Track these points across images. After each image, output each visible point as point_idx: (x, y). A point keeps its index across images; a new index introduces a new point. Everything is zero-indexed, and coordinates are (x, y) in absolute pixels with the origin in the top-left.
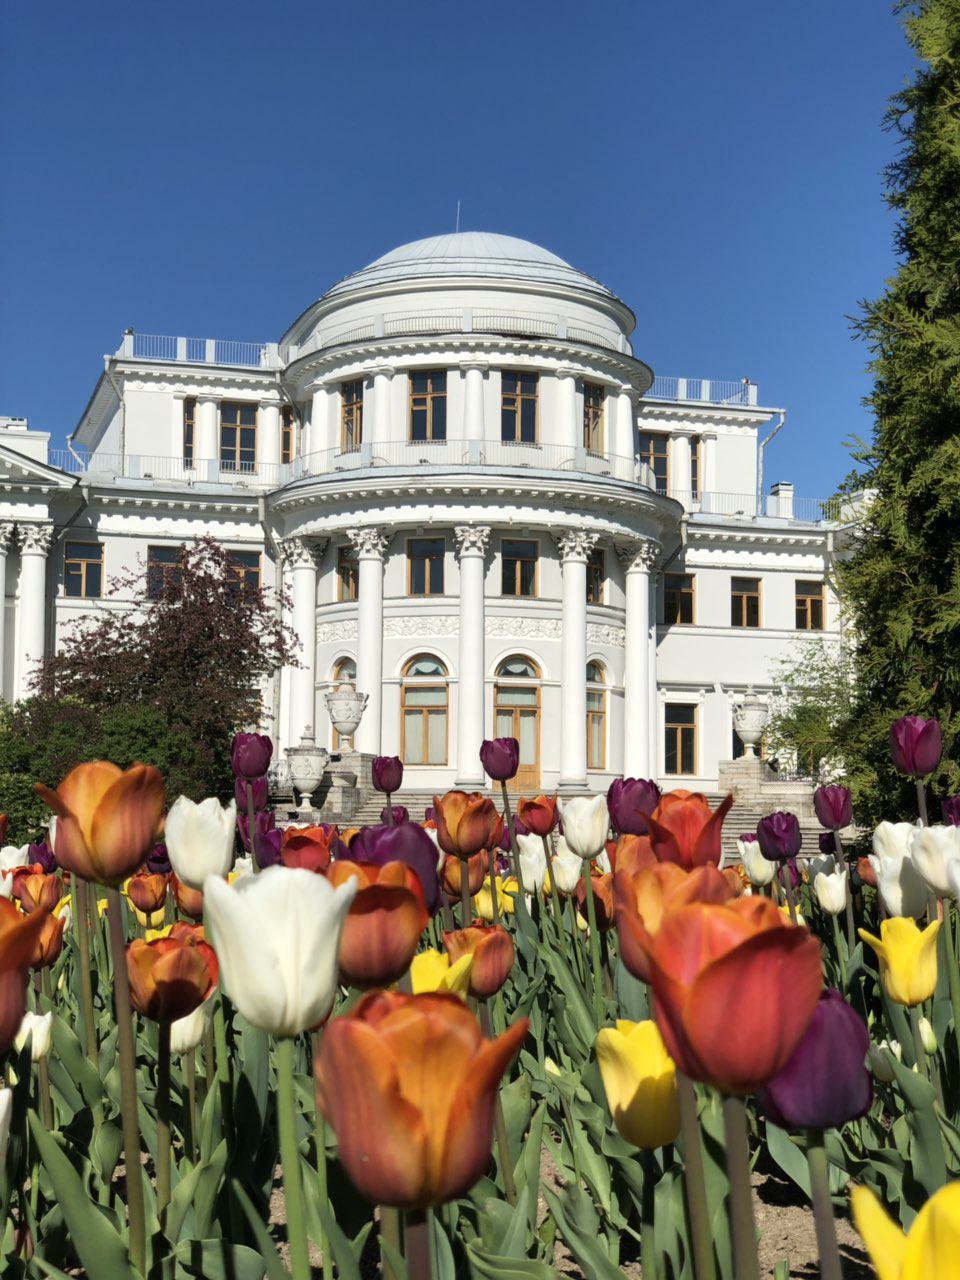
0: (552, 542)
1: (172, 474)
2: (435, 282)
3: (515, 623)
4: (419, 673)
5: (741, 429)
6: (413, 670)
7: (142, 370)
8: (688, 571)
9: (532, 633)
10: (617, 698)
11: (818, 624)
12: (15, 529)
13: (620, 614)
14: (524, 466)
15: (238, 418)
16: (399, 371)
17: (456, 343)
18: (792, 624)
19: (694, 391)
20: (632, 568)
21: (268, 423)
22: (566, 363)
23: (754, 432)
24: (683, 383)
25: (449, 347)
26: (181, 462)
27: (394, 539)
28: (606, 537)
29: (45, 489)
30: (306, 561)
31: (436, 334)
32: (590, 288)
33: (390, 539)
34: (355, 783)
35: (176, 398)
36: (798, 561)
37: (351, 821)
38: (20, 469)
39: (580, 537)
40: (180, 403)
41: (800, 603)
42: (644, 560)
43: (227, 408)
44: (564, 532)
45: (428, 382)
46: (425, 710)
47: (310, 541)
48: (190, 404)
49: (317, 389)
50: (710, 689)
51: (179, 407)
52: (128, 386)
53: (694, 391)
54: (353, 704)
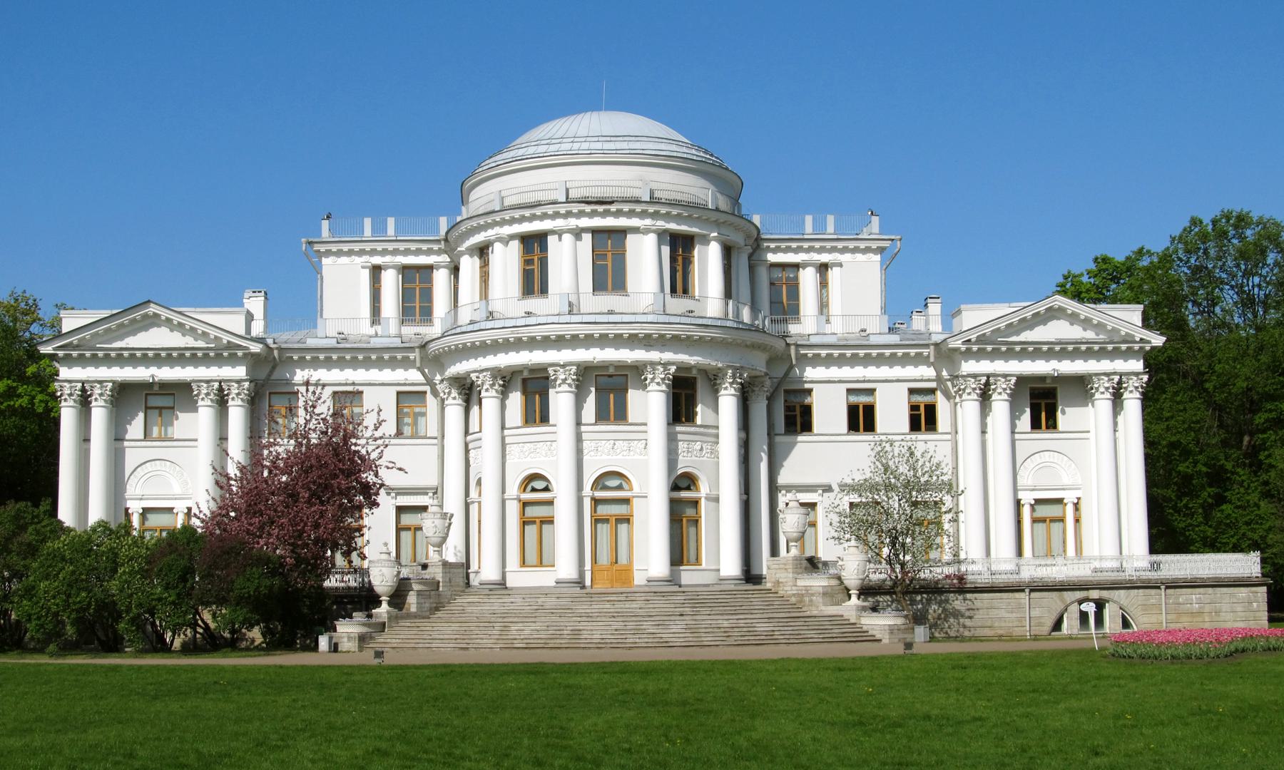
0: (632, 375)
1: (362, 328)
2: (555, 160)
3: (609, 445)
4: (534, 490)
5: (865, 256)
6: (529, 488)
7: (334, 248)
8: (807, 386)
9: (625, 453)
10: (712, 504)
12: (220, 386)
13: (713, 431)
14: (611, 312)
16: (512, 237)
17: (550, 212)
18: (906, 426)
19: (820, 225)
20: (723, 392)
21: (441, 279)
22: (648, 222)
23: (878, 258)
24: (809, 220)
25: (544, 216)
26: (368, 322)
27: (507, 380)
28: (682, 368)
29: (240, 353)
30: (454, 398)
31: (538, 204)
32: (675, 154)
33: (507, 379)
34: (438, 587)
35: (363, 267)
36: (910, 371)
37: (429, 618)
38: (221, 339)
39: (658, 370)
40: (367, 272)
41: (914, 408)
42: (731, 384)
43: (406, 271)
45: (534, 244)
46: (538, 521)
48: (376, 271)
49: (462, 254)
50: (828, 489)
51: (365, 275)
52: (324, 261)
53: (820, 225)
54: (438, 522)
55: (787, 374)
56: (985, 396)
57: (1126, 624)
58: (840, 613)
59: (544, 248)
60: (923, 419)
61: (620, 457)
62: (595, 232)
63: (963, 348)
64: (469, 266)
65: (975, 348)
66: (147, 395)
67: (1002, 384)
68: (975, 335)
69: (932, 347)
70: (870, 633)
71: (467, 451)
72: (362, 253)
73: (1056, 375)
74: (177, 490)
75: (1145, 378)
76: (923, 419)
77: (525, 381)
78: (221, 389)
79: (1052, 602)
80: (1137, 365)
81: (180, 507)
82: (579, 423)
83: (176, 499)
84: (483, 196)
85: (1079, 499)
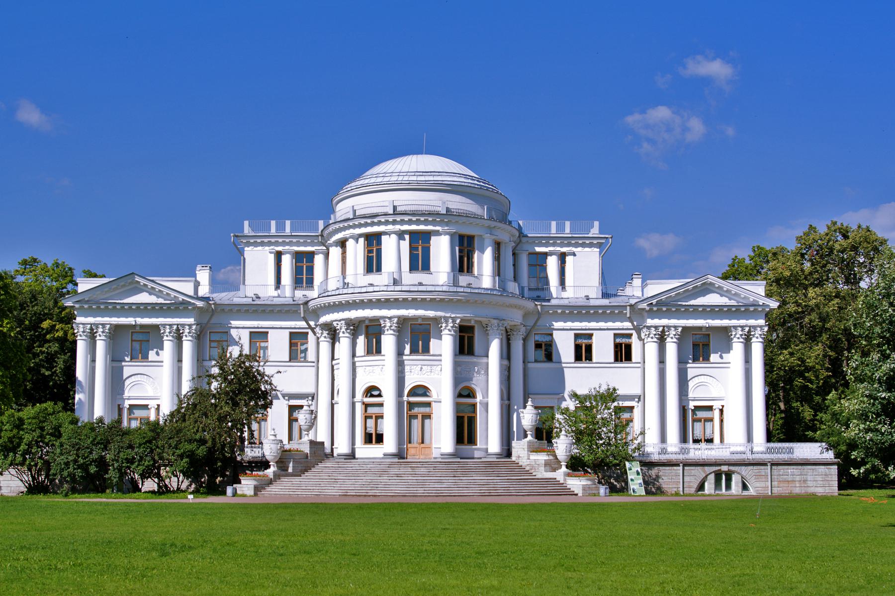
1: (269, 292)
9: (429, 374)
11: (628, 358)
12: (178, 327)
15: (303, 263)
16: (360, 236)
17: (383, 220)
25: (379, 223)
26: (273, 287)
27: (355, 327)
33: (356, 325)
35: (271, 253)
40: (273, 255)
43: (299, 257)
44: (436, 320)
48: (279, 256)
51: (271, 258)
55: (535, 323)
56: (662, 340)
57: (745, 487)
58: (555, 477)
59: (379, 243)
60: (623, 353)
61: (425, 376)
62: (412, 233)
63: (648, 308)
64: (335, 252)
65: (655, 309)
66: (132, 332)
67: (673, 332)
68: (656, 300)
69: (628, 307)
70: (571, 490)
71: (333, 370)
72: (270, 244)
73: (707, 326)
74: (150, 393)
76: (623, 353)
77: (367, 327)
78: (178, 330)
79: (698, 473)
81: (152, 404)
82: (354, 355)
83: (150, 399)
84: (343, 209)
85: (723, 406)
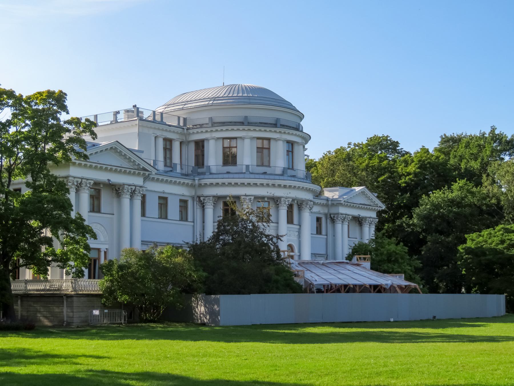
43: (165, 140)
47: (218, 198)
75: (377, 220)
80: (374, 215)
